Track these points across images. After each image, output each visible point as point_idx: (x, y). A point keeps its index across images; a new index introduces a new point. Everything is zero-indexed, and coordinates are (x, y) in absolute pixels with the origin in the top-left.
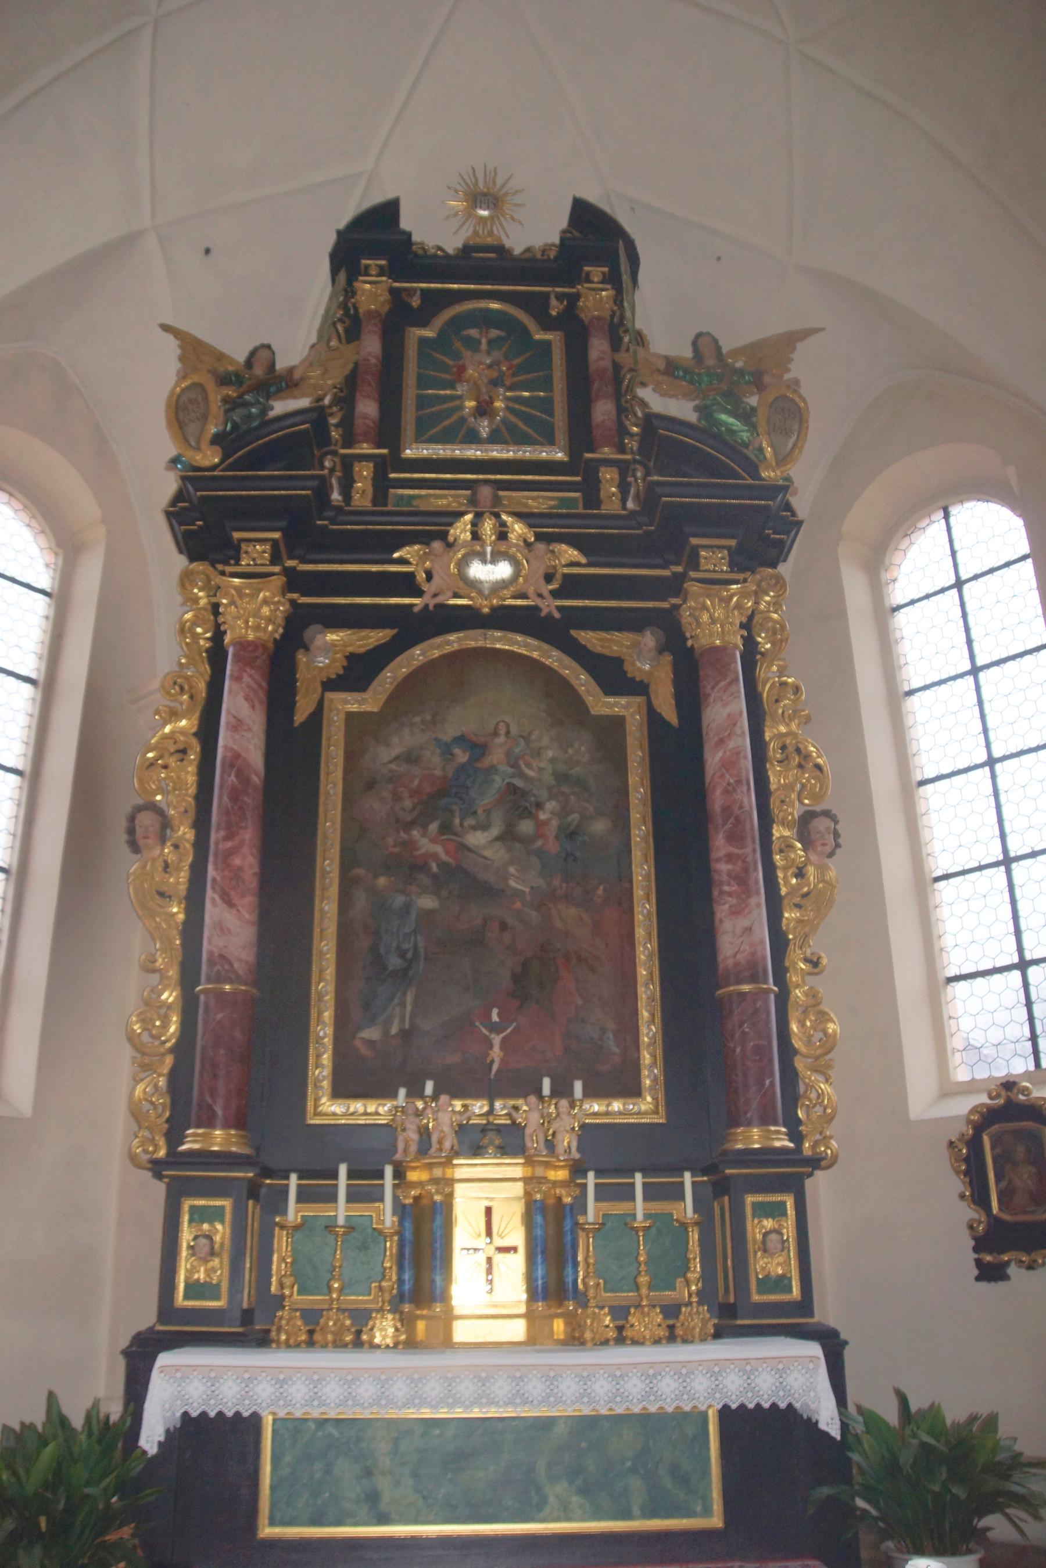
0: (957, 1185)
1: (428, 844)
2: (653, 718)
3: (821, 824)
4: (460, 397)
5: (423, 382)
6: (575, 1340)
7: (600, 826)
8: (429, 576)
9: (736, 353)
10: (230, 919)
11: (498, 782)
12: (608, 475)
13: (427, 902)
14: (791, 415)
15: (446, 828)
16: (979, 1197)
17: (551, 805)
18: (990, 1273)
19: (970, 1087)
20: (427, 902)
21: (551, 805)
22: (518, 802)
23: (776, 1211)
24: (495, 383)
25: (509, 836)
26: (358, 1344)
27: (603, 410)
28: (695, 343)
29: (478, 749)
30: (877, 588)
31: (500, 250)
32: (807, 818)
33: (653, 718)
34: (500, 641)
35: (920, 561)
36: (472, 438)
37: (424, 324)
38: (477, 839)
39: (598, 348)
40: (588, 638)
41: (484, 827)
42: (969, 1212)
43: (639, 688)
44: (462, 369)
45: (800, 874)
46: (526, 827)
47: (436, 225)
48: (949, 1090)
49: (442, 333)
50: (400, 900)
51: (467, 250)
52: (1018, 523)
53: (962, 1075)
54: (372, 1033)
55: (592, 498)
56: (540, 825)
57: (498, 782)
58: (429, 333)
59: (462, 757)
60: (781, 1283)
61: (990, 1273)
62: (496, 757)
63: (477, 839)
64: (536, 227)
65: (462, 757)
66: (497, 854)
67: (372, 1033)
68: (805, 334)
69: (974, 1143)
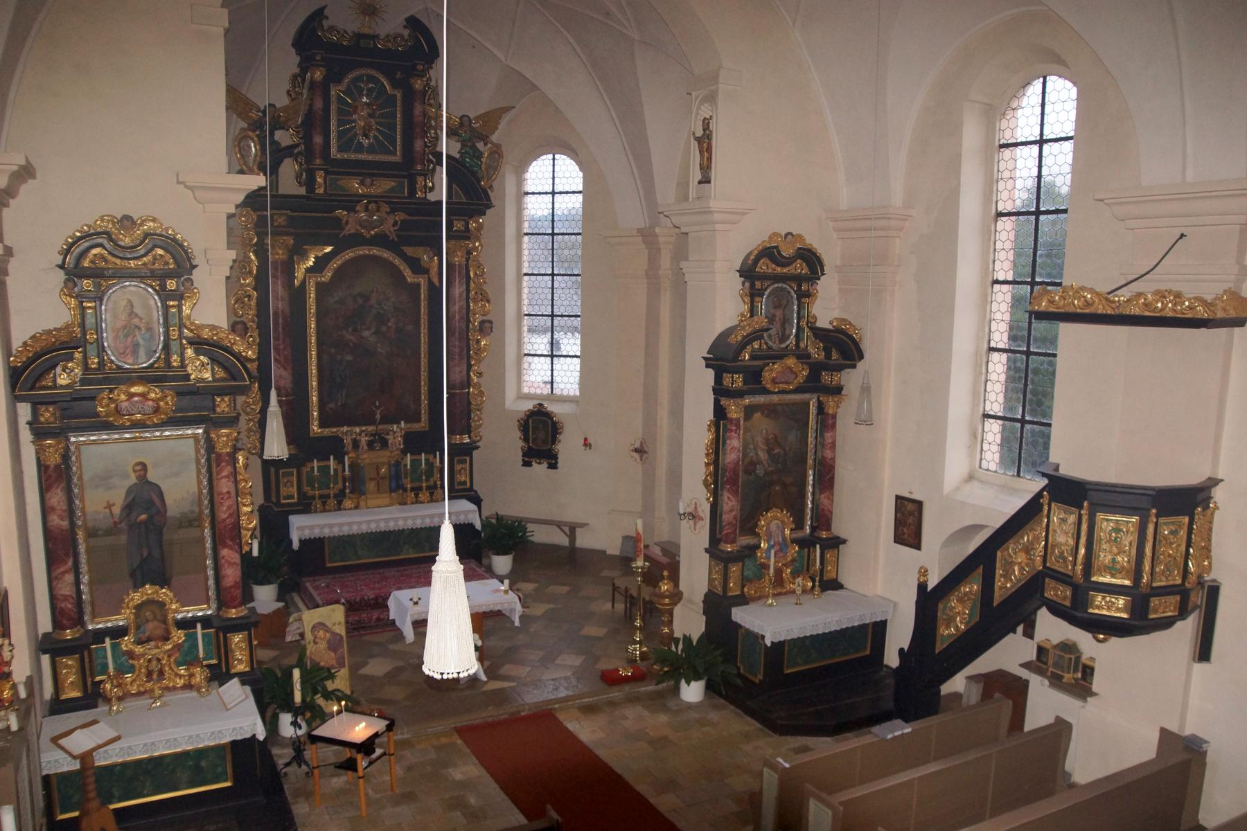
0: (518, 434)
1: (348, 337)
2: (431, 283)
3: (487, 325)
4: (354, 121)
5: (340, 112)
6: (404, 503)
7: (410, 328)
8: (347, 223)
9: (478, 118)
10: (284, 373)
11: (374, 311)
12: (420, 179)
13: (349, 358)
14: (497, 152)
15: (355, 330)
16: (526, 439)
17: (393, 320)
18: (527, 464)
19: (529, 397)
20: (349, 358)
21: (393, 320)
22: (381, 319)
23: (464, 462)
24: (370, 116)
25: (377, 333)
26: (340, 509)
27: (418, 145)
28: (461, 118)
29: (367, 298)
30: (520, 181)
31: (374, 37)
32: (482, 323)
33: (431, 283)
34: (375, 251)
35: (538, 173)
36: (360, 148)
37: (339, 81)
38: (366, 334)
39: (418, 109)
40: (409, 251)
41: (369, 329)
42: (521, 444)
43: (426, 271)
44: (356, 108)
45: (478, 342)
46: (384, 329)
47: (344, 20)
48: (522, 397)
49: (348, 88)
50: (339, 357)
51: (359, 36)
52: (581, 174)
53: (526, 390)
54: (332, 405)
55: (412, 192)
56: (389, 328)
57: (374, 311)
58: (343, 87)
59: (360, 301)
60: (465, 483)
61: (527, 464)
62: (373, 301)
63: (366, 334)
64: (390, 25)
65: (360, 301)
66: (373, 339)
67: (332, 405)
68: (506, 110)
69: (526, 421)
